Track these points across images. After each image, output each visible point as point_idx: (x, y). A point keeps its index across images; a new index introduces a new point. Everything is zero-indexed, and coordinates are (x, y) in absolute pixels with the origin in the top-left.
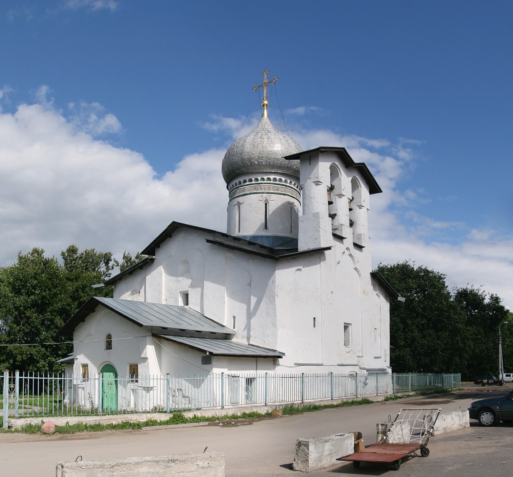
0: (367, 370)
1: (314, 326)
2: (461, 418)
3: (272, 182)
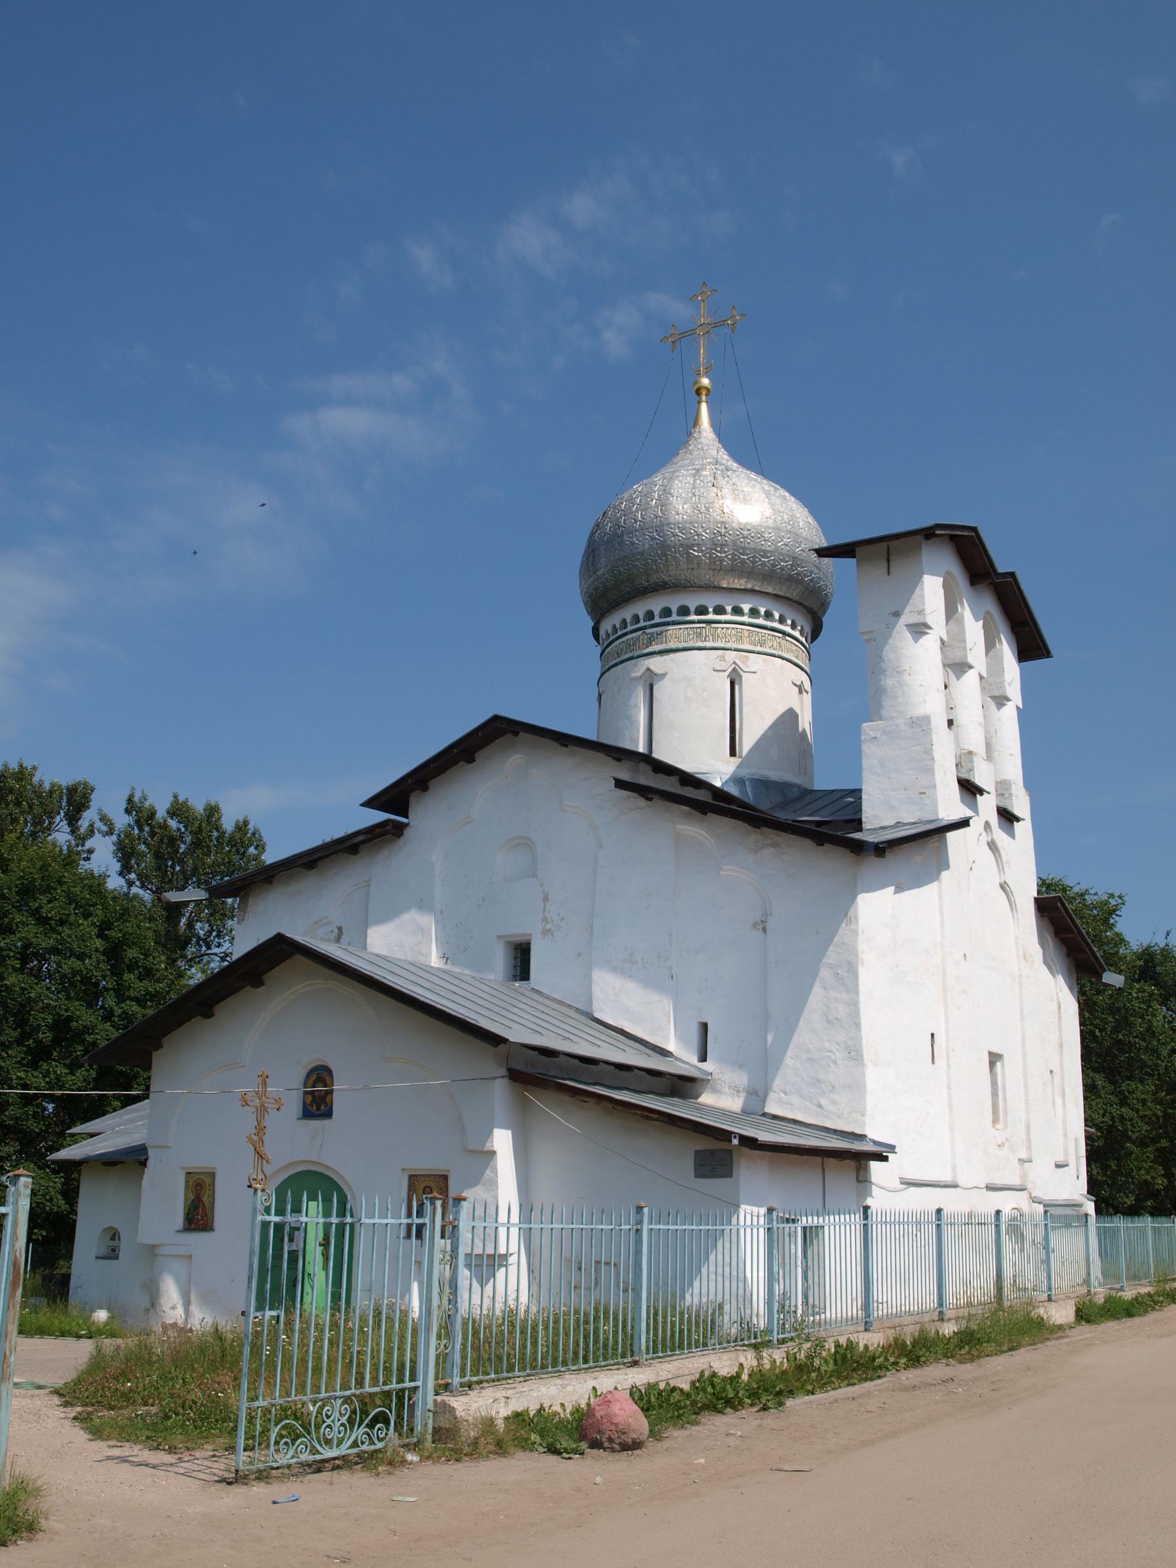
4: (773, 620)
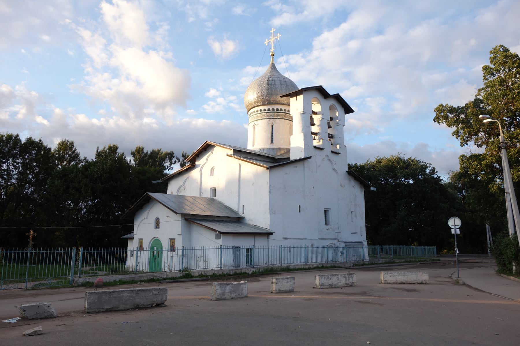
1: (300, 212)
2: (348, 279)
3: (275, 111)
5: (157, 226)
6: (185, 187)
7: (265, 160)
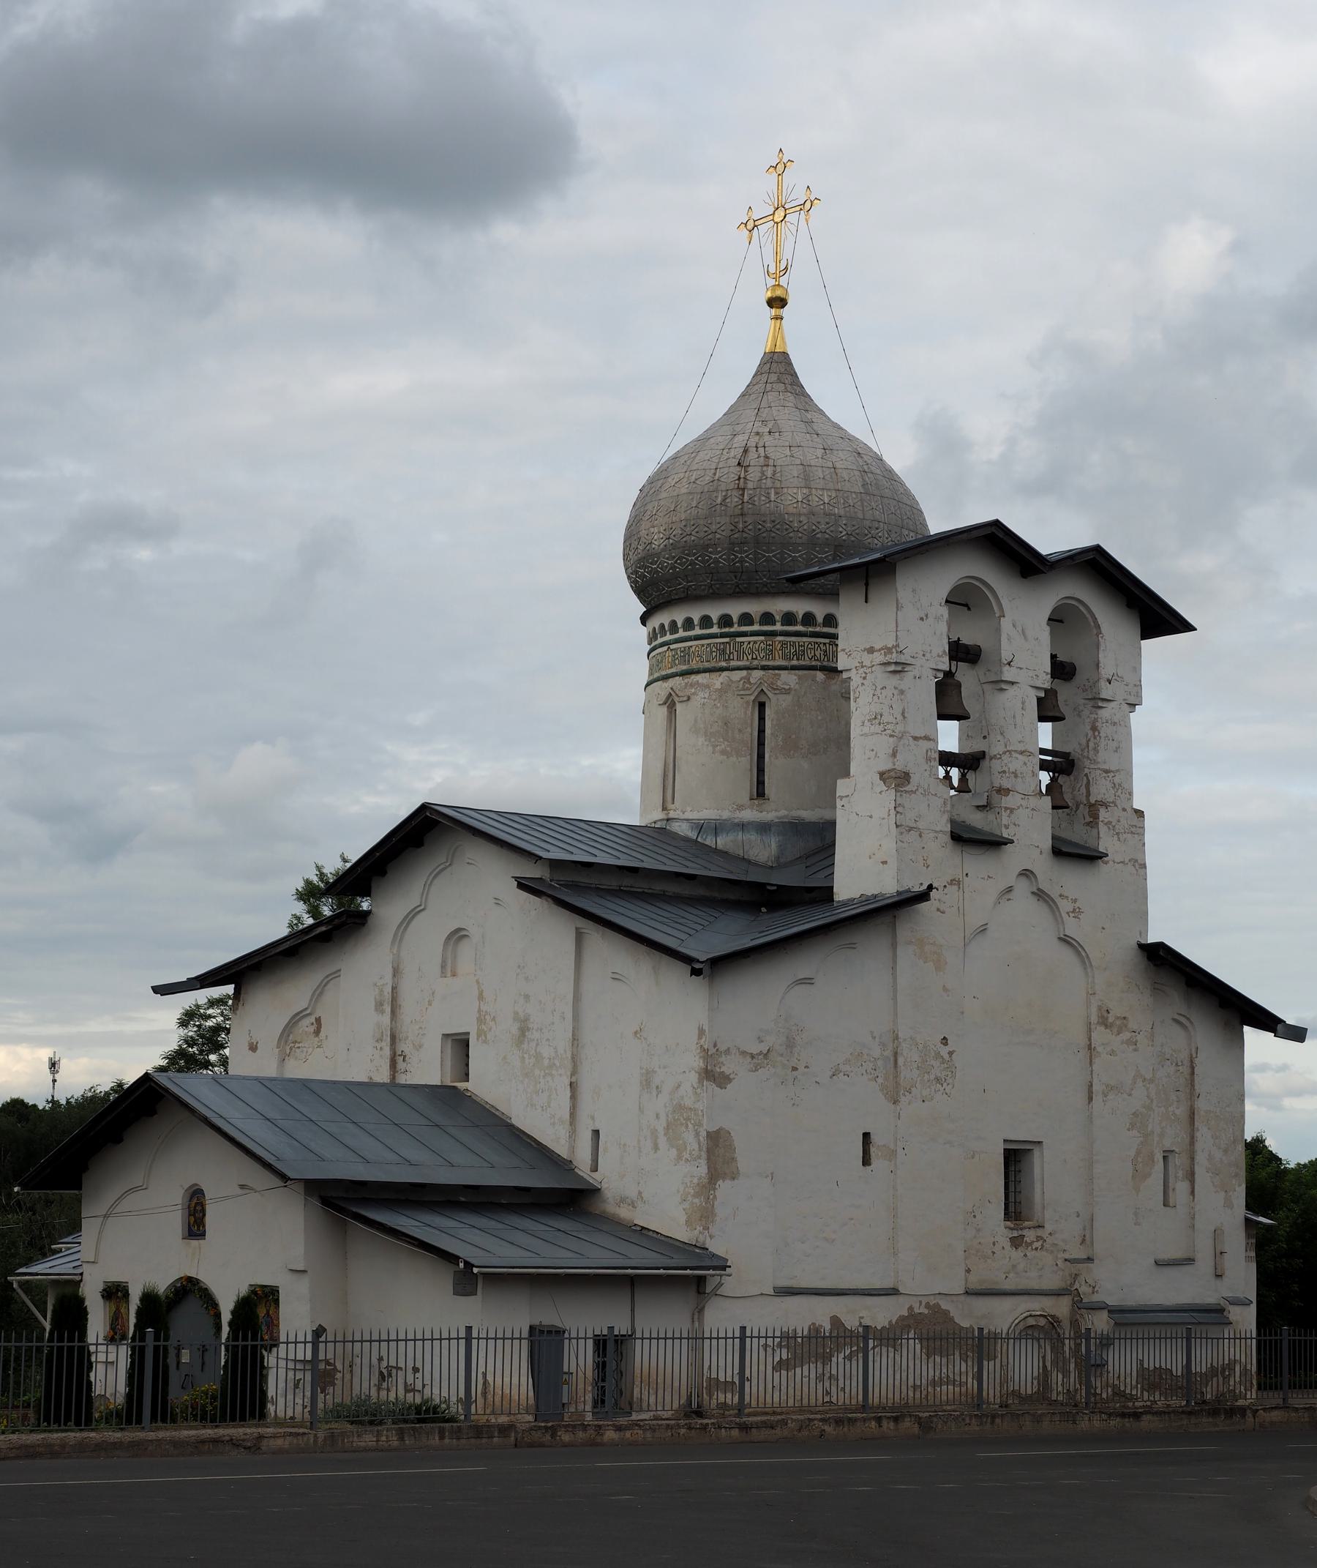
0: (1113, 1311)
1: (866, 1161)
3: (778, 627)
4: (815, 625)
5: (195, 1227)
6: (318, 1020)
7: (716, 894)
